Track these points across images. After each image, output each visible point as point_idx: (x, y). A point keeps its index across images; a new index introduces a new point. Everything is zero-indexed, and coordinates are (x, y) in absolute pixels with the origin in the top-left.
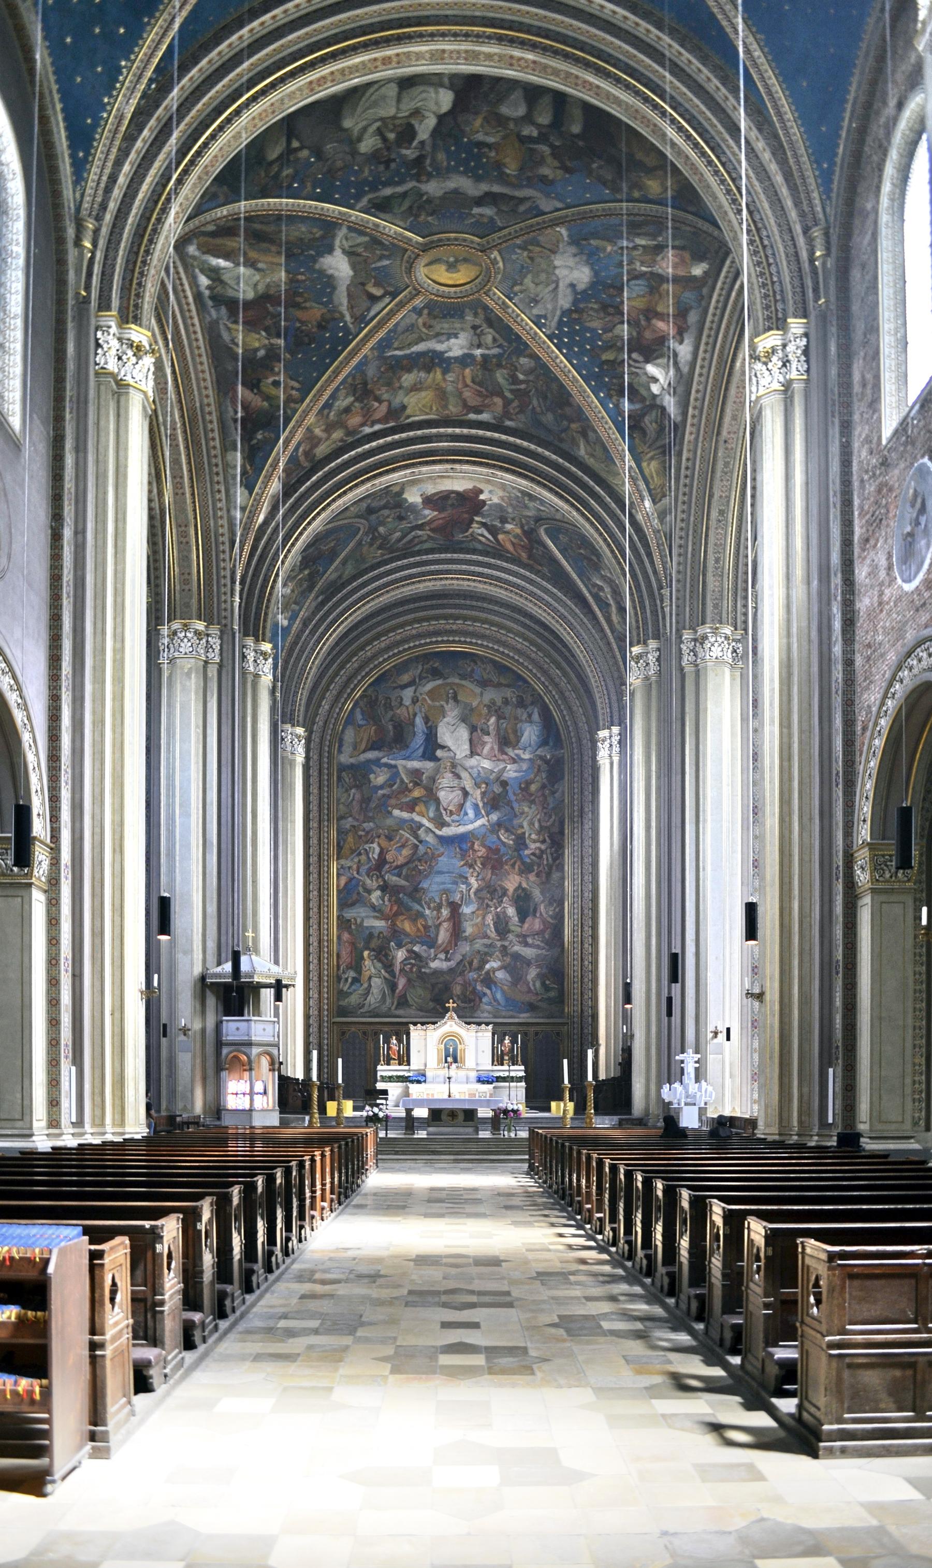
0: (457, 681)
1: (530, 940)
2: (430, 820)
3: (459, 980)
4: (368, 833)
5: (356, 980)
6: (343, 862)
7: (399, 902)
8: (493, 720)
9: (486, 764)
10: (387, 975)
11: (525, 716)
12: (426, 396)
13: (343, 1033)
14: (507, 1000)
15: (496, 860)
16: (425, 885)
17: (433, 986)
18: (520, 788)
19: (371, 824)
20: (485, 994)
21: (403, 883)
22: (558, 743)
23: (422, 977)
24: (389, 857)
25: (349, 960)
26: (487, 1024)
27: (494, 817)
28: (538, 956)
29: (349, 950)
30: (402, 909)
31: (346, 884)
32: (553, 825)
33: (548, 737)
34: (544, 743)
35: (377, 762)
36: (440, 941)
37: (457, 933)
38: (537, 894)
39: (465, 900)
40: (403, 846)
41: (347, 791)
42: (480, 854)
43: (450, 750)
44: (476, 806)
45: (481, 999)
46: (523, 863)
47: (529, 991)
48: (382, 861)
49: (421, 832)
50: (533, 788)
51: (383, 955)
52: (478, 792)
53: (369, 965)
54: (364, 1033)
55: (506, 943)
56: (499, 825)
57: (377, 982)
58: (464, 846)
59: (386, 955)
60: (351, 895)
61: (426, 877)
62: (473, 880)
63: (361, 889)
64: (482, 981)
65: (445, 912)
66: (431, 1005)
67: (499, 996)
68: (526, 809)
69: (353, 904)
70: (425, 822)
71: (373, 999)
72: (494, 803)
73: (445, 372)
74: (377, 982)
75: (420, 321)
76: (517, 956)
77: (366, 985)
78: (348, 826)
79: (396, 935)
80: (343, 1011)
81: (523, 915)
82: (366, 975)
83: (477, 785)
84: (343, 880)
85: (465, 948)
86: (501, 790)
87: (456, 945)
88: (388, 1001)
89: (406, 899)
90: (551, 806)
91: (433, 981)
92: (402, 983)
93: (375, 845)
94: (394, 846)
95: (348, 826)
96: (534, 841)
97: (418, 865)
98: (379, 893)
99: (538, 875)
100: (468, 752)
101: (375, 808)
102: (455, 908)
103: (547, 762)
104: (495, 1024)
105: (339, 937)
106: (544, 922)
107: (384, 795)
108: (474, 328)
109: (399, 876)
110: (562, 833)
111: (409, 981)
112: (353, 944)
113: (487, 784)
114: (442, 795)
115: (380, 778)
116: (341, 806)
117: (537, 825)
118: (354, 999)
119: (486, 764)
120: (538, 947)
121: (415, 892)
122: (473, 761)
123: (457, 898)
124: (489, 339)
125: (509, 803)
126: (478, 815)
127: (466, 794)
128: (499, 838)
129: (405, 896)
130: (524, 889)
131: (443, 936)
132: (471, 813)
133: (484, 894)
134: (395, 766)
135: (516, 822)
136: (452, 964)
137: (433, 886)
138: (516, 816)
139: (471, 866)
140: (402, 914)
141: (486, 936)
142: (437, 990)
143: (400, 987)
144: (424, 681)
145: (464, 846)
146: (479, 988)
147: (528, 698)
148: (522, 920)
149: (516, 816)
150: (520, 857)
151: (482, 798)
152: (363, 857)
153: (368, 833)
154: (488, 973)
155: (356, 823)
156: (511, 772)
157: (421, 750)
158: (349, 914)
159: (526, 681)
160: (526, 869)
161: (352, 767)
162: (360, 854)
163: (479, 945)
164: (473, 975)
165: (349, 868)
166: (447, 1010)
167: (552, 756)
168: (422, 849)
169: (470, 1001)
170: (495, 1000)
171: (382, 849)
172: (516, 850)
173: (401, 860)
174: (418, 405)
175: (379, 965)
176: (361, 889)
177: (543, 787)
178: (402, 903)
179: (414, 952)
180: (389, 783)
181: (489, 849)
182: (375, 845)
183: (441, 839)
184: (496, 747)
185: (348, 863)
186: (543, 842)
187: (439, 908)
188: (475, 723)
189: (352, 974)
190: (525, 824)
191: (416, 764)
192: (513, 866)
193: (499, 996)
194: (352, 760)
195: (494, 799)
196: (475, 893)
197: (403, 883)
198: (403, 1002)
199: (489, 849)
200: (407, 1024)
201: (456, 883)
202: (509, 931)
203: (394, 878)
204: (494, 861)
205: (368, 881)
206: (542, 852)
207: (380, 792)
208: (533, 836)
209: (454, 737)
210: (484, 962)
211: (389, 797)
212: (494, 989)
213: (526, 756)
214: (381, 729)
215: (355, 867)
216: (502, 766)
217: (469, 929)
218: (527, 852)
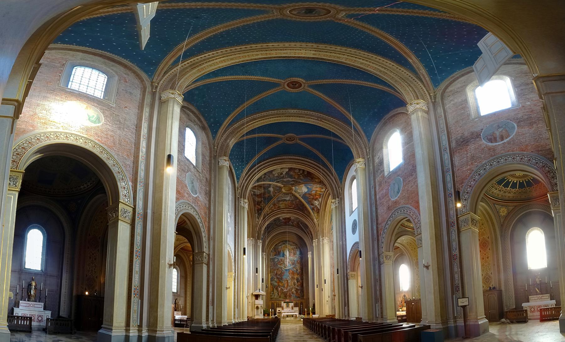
12: (283, 205)
30: (280, 281)
37: (288, 285)
51: (277, 289)
60: (272, 279)
72: (293, 264)
85: (289, 288)
97: (282, 274)
115: (276, 260)
121: (282, 279)
129: (280, 279)
131: (286, 286)
137: (284, 277)
156: (295, 259)
160: (298, 274)
174: (282, 206)
183: (286, 270)
204: (293, 273)
209: (287, 253)
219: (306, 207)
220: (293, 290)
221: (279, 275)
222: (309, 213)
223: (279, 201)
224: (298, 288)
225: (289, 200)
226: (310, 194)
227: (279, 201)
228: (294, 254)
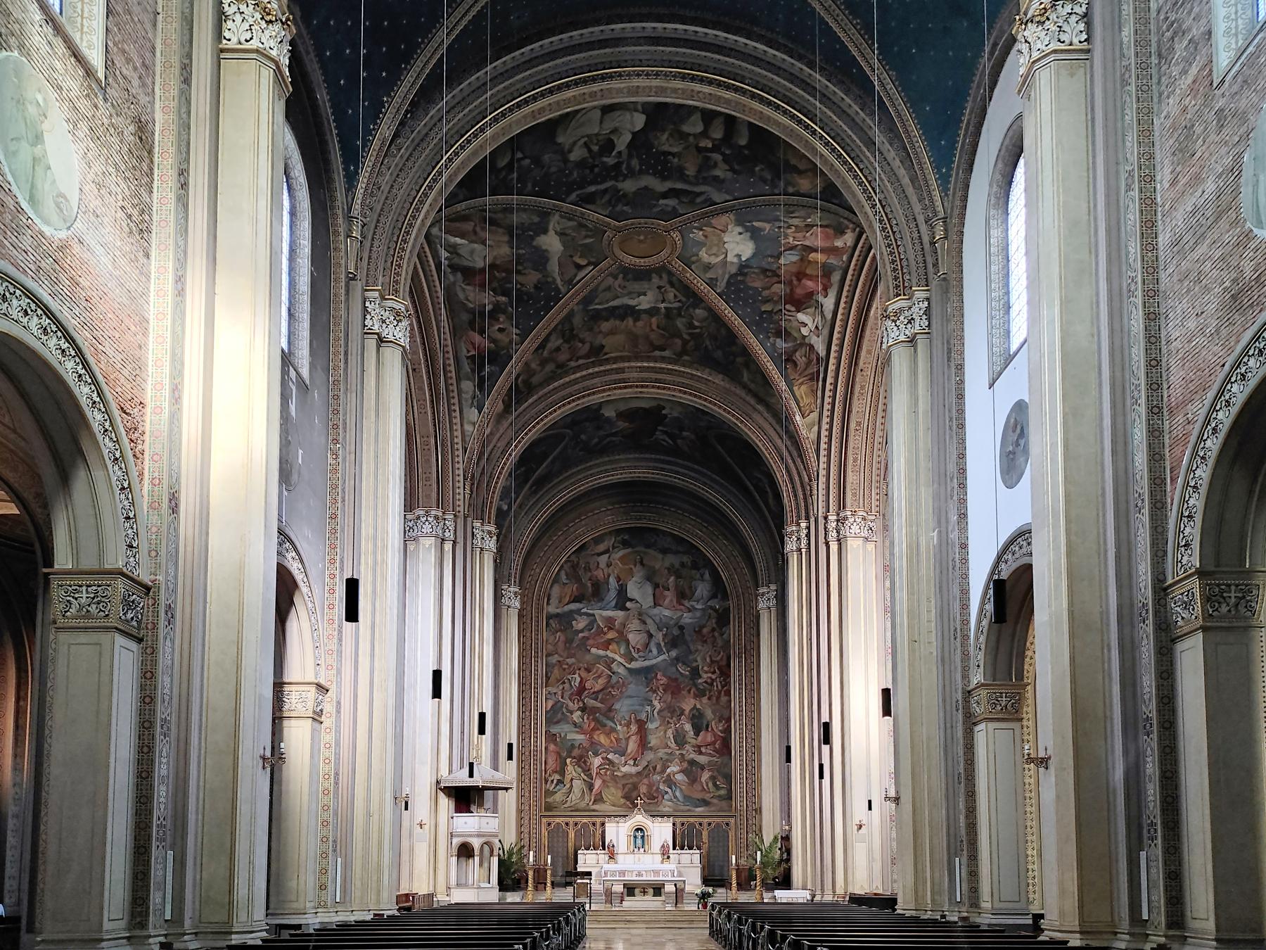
1: (703, 750)
2: (621, 656)
3: (645, 781)
5: (559, 782)
6: (549, 689)
13: (549, 824)
16: (617, 706)
17: (624, 786)
21: (599, 705)
23: (614, 778)
24: (588, 685)
26: (669, 816)
27: (674, 653)
30: (600, 725)
37: (643, 745)
38: (709, 714)
39: (650, 718)
40: (599, 677)
44: (658, 645)
46: (698, 689)
48: (582, 689)
51: (582, 761)
53: (571, 770)
54: (567, 824)
56: (677, 659)
57: (578, 784)
59: (585, 762)
60: (555, 715)
61: (618, 700)
62: (656, 703)
65: (634, 728)
66: (623, 801)
67: (678, 794)
69: (557, 722)
70: (619, 659)
71: (575, 797)
73: (636, 320)
74: (577, 783)
75: (617, 283)
76: (692, 763)
79: (594, 747)
80: (549, 807)
82: (568, 778)
84: (550, 703)
85: (650, 756)
88: (587, 797)
89: (602, 718)
91: (624, 782)
92: (598, 783)
94: (591, 676)
99: (709, 699)
102: (641, 725)
106: (715, 735)
108: (659, 288)
111: (604, 781)
112: (558, 754)
118: (558, 797)
121: (609, 712)
123: (643, 716)
124: (671, 296)
126: (660, 652)
130: (698, 710)
132: (655, 651)
133: (666, 713)
135: (691, 657)
136: (640, 768)
137: (623, 707)
139: (655, 692)
141: (667, 746)
143: (596, 787)
148: (697, 734)
149: (691, 652)
150: (695, 685)
152: (567, 685)
158: (555, 730)
160: (700, 694)
163: (661, 753)
168: (614, 679)
169: (654, 798)
170: (675, 797)
173: (598, 687)
181: (669, 678)
185: (553, 690)
186: (714, 673)
187: (628, 725)
189: (557, 777)
192: (689, 691)
197: (599, 705)
198: (599, 799)
201: (643, 705)
204: (674, 688)
210: (665, 768)
217: (653, 741)
219: (745, 352)
220: (673, 768)
221: (595, 695)
222: (766, 381)
223: (597, 317)
224: (702, 759)
225: (652, 312)
226: (771, 274)
227: (597, 317)
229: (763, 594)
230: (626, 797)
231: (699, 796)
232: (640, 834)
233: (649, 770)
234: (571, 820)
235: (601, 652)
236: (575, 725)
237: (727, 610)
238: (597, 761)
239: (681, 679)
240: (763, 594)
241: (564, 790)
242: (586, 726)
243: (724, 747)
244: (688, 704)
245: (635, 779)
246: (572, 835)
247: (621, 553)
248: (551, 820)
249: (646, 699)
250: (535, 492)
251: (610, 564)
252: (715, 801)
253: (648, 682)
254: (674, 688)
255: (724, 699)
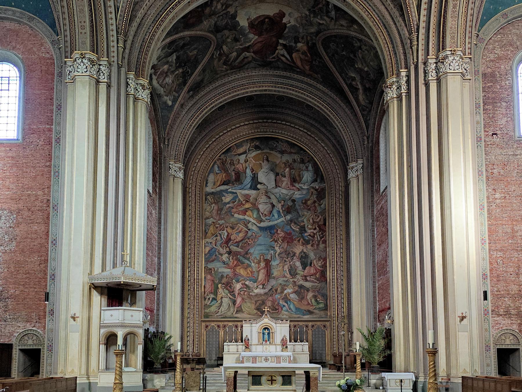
0: (269, 151)
1: (308, 278)
3: (270, 298)
4: (221, 225)
5: (214, 299)
6: (207, 240)
7: (238, 260)
8: (287, 169)
9: (284, 191)
10: (231, 297)
11: (304, 167)
13: (207, 327)
14: (296, 308)
15: (290, 238)
16: (251, 251)
17: (256, 302)
18: (302, 203)
19: (223, 221)
20: (284, 306)
22: (322, 180)
24: (232, 238)
25: (210, 289)
27: (288, 217)
28: (312, 286)
29: (210, 284)
31: (209, 251)
32: (320, 220)
33: (317, 177)
34: (315, 181)
35: (226, 191)
36: (259, 279)
37: (269, 275)
38: (312, 255)
39: (273, 258)
40: (240, 232)
41: (210, 205)
42: (281, 235)
43: (264, 185)
45: (282, 309)
46: (304, 240)
47: (309, 304)
48: (228, 240)
49: (250, 226)
50: (309, 203)
51: (228, 286)
52: (280, 206)
53: (222, 292)
54: (219, 326)
55: (295, 280)
56: (291, 221)
57: (226, 301)
58: (272, 232)
59: (230, 287)
61: (252, 247)
62: (277, 248)
63: (217, 253)
64: (282, 299)
65: (263, 264)
66: (255, 311)
67: (292, 306)
68: (306, 213)
69: (213, 261)
74: (226, 301)
76: (301, 287)
77: (219, 302)
78: (210, 222)
80: (207, 316)
81: (304, 266)
82: (219, 297)
83: (279, 202)
84: (207, 249)
85: (273, 282)
86: (292, 204)
87: (268, 281)
88: (232, 309)
89: (241, 258)
90: (319, 211)
91: (256, 299)
92: (239, 300)
93: (225, 231)
95: (210, 222)
96: (310, 229)
98: (227, 255)
99: (312, 246)
100: (274, 186)
101: (226, 212)
102: (268, 263)
103: (316, 190)
104: (291, 321)
105: (205, 278)
107: (230, 207)
109: (238, 247)
110: (325, 224)
111: (243, 299)
113: (284, 201)
114: (261, 207)
115: (227, 198)
116: (207, 212)
117: (311, 221)
118: (213, 309)
119: (284, 191)
120: (313, 282)
122: (277, 190)
123: (269, 257)
125: (296, 210)
126: (280, 216)
127: (273, 206)
128: (291, 228)
130: (304, 253)
132: (276, 216)
133: (283, 255)
134: (236, 193)
135: (300, 219)
136: (266, 290)
137: (256, 252)
138: (300, 216)
139: (276, 241)
140: (239, 266)
142: (258, 304)
144: (251, 152)
145: (272, 232)
146: (281, 302)
147: (306, 159)
148: (304, 268)
149: (300, 216)
151: (282, 208)
153: (221, 225)
154: (286, 295)
155: (215, 221)
156: (297, 195)
157: (249, 186)
158: (210, 266)
159: (305, 151)
160: (306, 242)
161: (212, 193)
162: (217, 236)
163: (281, 281)
164: (277, 296)
165: (211, 243)
166: (263, 312)
167: (319, 187)
168: (250, 233)
169: (276, 309)
171: (228, 233)
172: (300, 233)
173: (239, 239)
175: (227, 291)
176: (217, 253)
177: (315, 202)
178: (239, 260)
179: (246, 285)
180: (233, 201)
181: (286, 233)
182: (225, 231)
183: (261, 228)
184: (289, 183)
185: (209, 240)
186: (315, 229)
187: (259, 262)
188: (278, 171)
189: (212, 296)
190: (305, 220)
191: (247, 192)
192: (299, 241)
193: (292, 306)
194: (213, 190)
195: (288, 208)
196: (278, 255)
197: (239, 250)
198: (239, 310)
199: (286, 233)
200: (242, 321)
202: (297, 274)
203: (235, 248)
204: (289, 239)
205: (221, 249)
206: (314, 234)
207: (228, 205)
208: (309, 226)
211: (233, 208)
212: (289, 303)
213: (306, 187)
214: (228, 175)
215: (214, 242)
216: (292, 192)
217: (275, 273)
218: (306, 234)
220: (288, 290)
224: (307, 285)
228: (294, 180)
229: (352, 168)
230: (258, 309)
231: (306, 308)
232: (266, 332)
233: (273, 291)
234: (221, 324)
235: (241, 217)
236: (224, 262)
237: (323, 190)
238: (238, 286)
239: (293, 233)
240: (352, 168)
241: (217, 304)
242: (231, 264)
243: (323, 276)
244: (298, 249)
245: (263, 297)
246: (222, 333)
247: (254, 154)
248: (208, 324)
249: (271, 246)
250: (192, 97)
251: (247, 160)
252: (316, 311)
253: (272, 235)
254: (289, 239)
255: (322, 246)
